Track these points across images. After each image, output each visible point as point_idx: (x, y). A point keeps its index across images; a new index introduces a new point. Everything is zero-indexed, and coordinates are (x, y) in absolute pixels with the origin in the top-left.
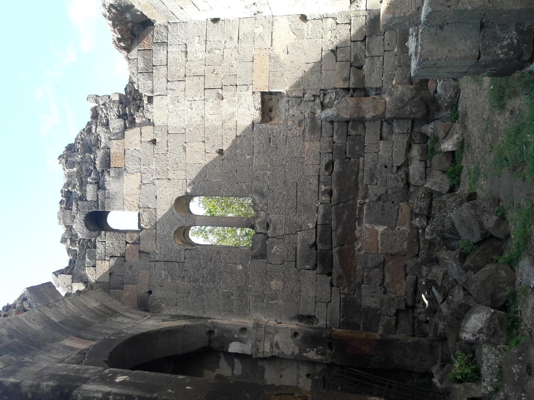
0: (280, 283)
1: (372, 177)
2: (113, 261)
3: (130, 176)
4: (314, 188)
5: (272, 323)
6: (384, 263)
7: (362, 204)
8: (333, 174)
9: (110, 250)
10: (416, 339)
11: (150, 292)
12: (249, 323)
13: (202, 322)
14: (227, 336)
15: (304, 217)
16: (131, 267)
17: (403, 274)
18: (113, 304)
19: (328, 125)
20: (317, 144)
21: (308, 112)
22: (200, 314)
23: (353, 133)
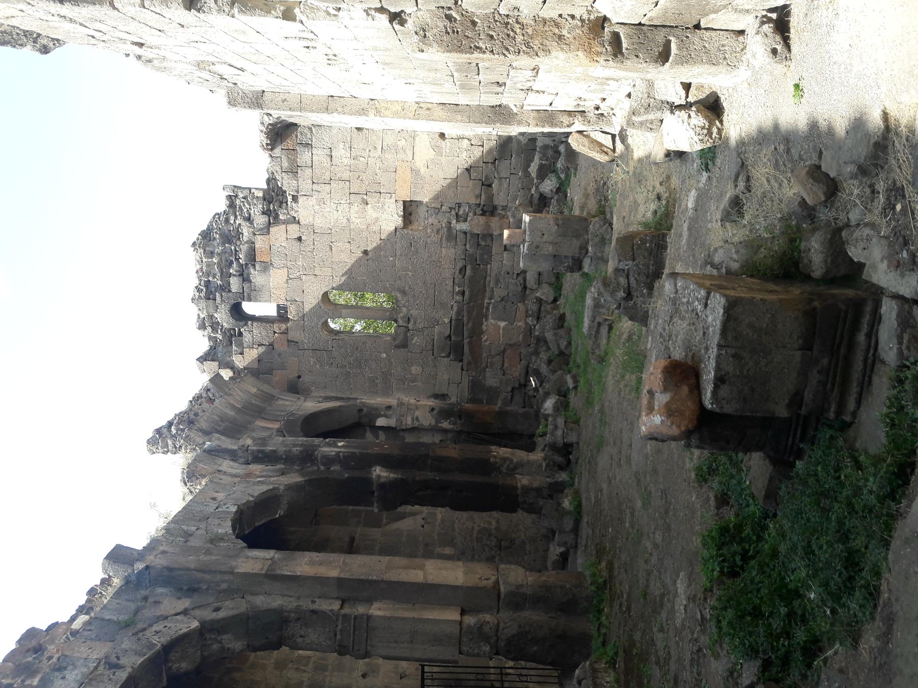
0: (420, 369)
1: (497, 282)
2: (261, 349)
3: (277, 271)
4: (450, 289)
5: (412, 401)
6: (504, 351)
7: (489, 304)
8: (466, 277)
9: (258, 339)
10: (526, 409)
11: (299, 377)
12: (393, 401)
13: (351, 402)
14: (375, 413)
15: (441, 313)
16: (279, 355)
17: (518, 360)
18: (266, 388)
19: (462, 235)
20: (453, 250)
21: (445, 221)
22: (347, 395)
23: (483, 243)
